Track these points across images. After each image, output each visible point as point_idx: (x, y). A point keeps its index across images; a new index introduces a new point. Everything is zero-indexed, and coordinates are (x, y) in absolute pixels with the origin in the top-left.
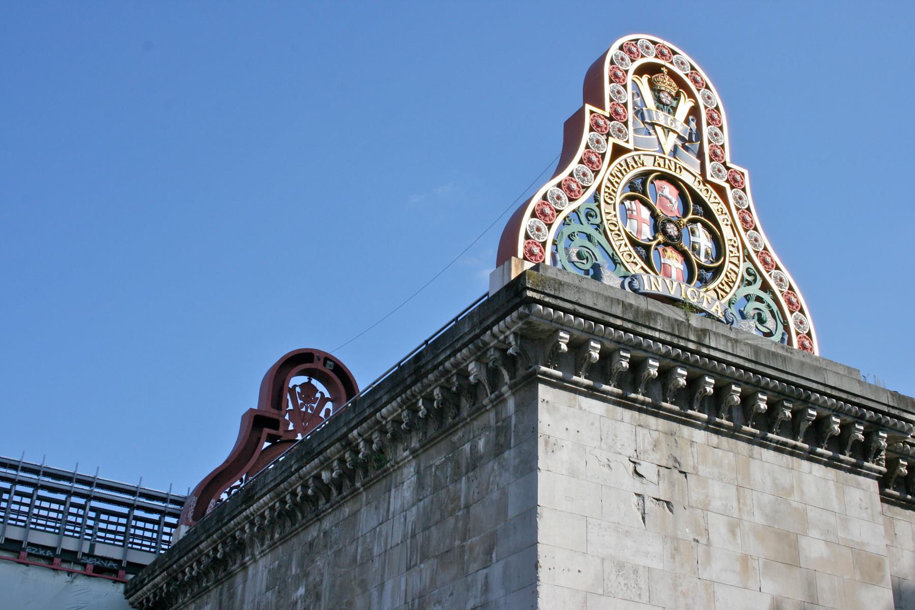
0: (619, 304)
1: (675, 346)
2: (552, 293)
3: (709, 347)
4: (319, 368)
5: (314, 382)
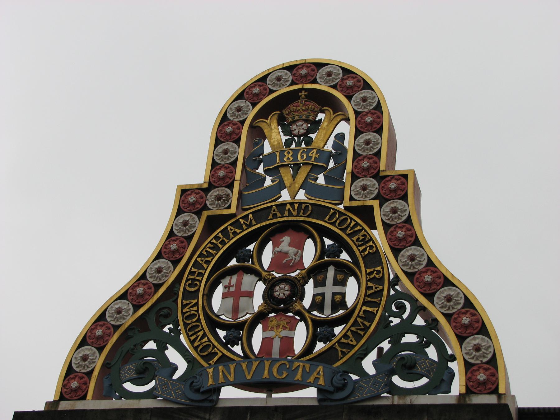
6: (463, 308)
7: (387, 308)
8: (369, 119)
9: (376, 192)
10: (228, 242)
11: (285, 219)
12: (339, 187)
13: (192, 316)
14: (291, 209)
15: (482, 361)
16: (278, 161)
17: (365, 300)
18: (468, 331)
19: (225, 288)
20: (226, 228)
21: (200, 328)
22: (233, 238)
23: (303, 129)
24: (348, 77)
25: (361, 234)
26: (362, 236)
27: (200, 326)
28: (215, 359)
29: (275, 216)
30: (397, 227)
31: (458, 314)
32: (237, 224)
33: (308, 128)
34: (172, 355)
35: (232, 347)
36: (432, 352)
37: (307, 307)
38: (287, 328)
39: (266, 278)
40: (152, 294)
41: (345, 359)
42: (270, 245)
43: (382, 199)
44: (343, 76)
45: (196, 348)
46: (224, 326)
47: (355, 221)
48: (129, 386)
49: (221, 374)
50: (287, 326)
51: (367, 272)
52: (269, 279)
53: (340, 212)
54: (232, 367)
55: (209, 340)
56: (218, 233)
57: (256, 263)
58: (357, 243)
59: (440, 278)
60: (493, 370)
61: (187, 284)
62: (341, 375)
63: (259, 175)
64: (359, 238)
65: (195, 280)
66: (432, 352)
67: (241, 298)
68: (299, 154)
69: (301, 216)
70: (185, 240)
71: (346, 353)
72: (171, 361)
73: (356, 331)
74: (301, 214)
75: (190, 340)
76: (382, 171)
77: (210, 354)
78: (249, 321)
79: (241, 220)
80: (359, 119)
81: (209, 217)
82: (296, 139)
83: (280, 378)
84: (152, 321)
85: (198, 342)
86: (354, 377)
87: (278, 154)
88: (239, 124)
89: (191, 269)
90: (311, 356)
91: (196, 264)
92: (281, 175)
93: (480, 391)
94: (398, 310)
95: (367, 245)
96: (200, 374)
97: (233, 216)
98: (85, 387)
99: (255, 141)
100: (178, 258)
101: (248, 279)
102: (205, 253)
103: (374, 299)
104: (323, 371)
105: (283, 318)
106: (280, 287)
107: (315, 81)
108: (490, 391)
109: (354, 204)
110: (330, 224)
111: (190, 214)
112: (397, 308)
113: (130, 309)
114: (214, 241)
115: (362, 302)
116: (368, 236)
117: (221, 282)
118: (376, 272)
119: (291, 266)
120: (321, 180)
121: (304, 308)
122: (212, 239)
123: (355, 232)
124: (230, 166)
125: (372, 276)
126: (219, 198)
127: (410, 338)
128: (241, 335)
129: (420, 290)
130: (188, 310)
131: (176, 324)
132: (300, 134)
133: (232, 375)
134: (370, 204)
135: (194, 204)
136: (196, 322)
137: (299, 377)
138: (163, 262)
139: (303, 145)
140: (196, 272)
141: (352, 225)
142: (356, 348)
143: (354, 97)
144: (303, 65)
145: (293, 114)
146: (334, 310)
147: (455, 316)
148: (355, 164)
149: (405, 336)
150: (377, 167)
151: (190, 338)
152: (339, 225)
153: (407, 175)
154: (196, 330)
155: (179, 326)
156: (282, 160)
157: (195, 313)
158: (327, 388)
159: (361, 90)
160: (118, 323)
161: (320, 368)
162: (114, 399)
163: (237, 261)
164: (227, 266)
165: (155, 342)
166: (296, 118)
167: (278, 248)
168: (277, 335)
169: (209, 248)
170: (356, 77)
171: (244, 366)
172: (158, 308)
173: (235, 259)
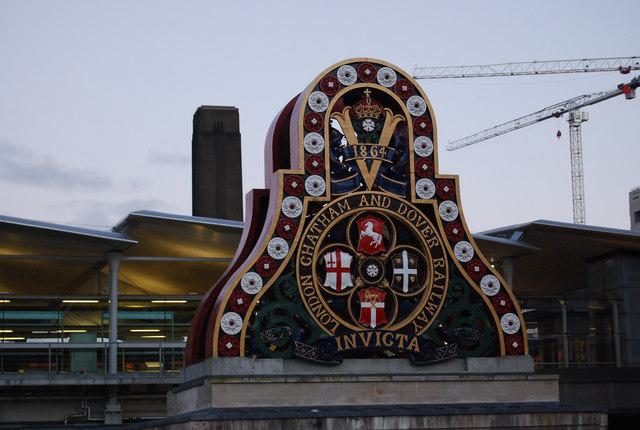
13: (310, 291)
54: (354, 336)
67: (343, 274)
81: (311, 204)
84: (277, 291)
91: (307, 241)
109: (418, 201)
156: (359, 154)
171: (362, 335)
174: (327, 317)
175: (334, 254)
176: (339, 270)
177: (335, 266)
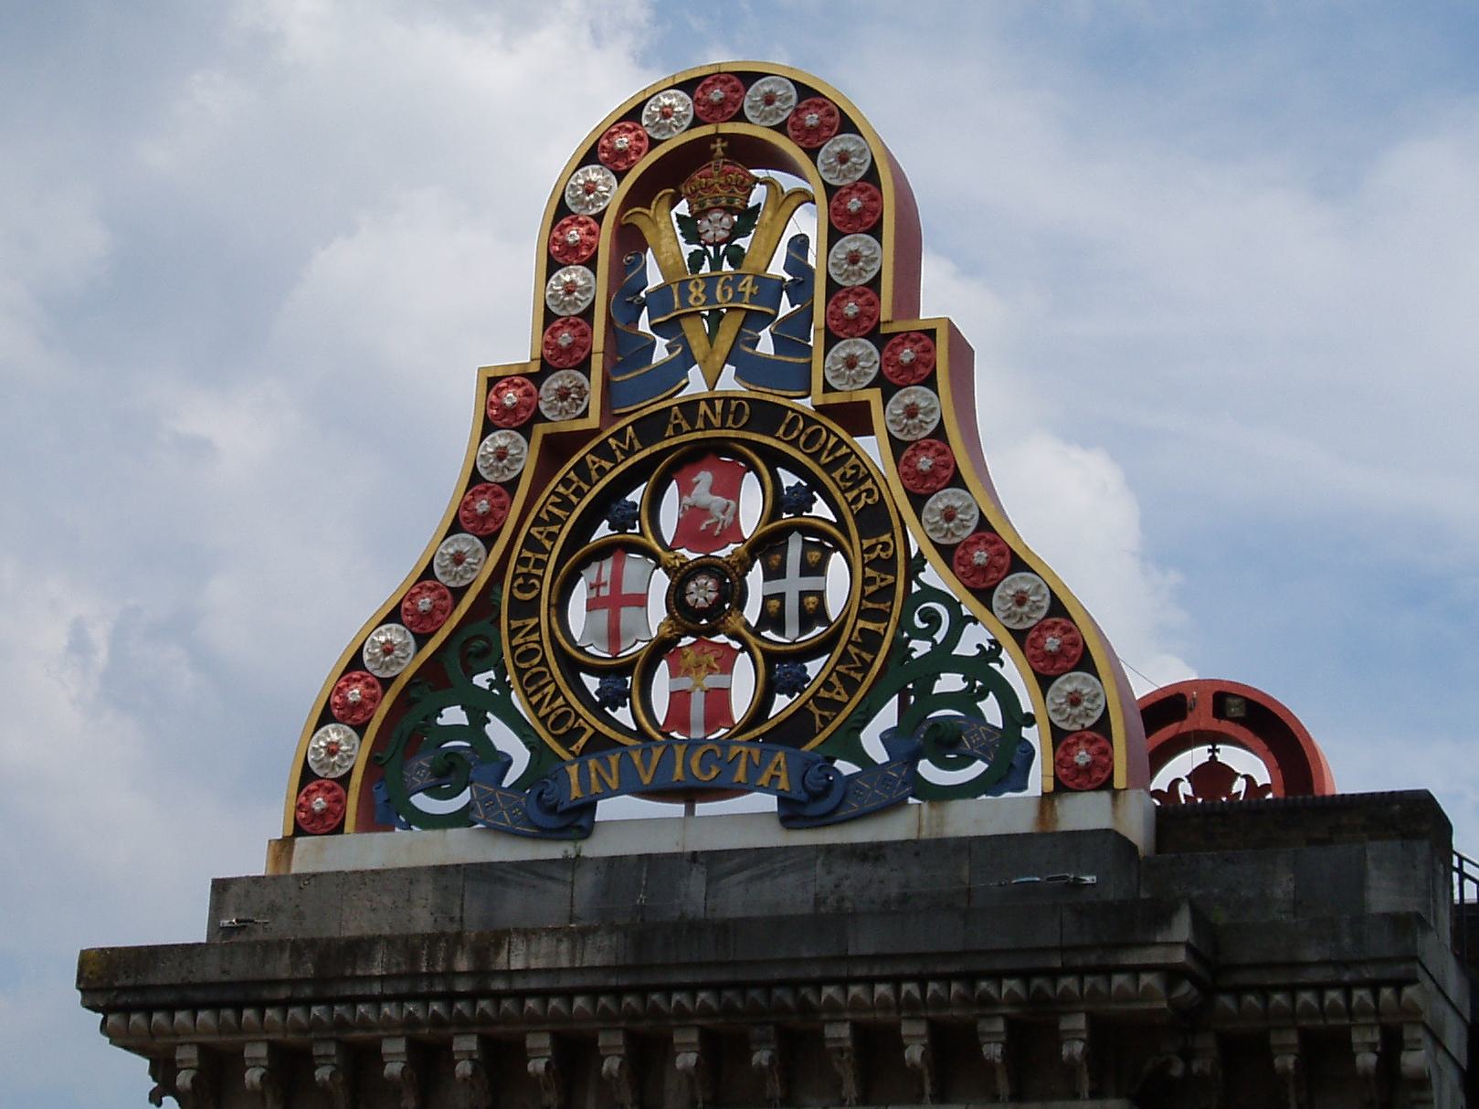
0: (282, 950)
1: (425, 999)
2: (130, 982)
3: (509, 974)
4: (1202, 725)
5: (1231, 756)
6: (1047, 617)
7: (904, 623)
8: (854, 204)
9: (874, 372)
10: (589, 491)
11: (699, 435)
12: (802, 360)
14: (709, 412)
15: (1083, 726)
16: (676, 306)
17: (862, 608)
18: (1058, 666)
19: (592, 588)
20: (583, 458)
21: (548, 678)
22: (598, 481)
23: (723, 229)
24: (809, 104)
25: (848, 464)
26: (852, 468)
27: (548, 674)
28: (582, 741)
29: (678, 430)
30: (917, 447)
31: (1039, 630)
32: (603, 451)
33: (734, 225)
34: (500, 734)
35: (614, 710)
36: (991, 709)
37: (753, 624)
38: (716, 669)
39: (669, 566)
40: (449, 611)
41: (827, 732)
42: (673, 488)
43: (886, 385)
44: (799, 101)
45: (543, 720)
46: (592, 671)
47: (836, 435)
48: (422, 801)
49: (593, 775)
50: (715, 665)
51: (865, 547)
52: (675, 566)
53: (806, 417)
55: (568, 704)
56: (568, 473)
57: (650, 535)
58: (841, 484)
59: (1003, 555)
60: (1104, 744)
61: (515, 585)
62: (820, 768)
63: (643, 336)
64: (845, 473)
65: (527, 576)
66: (991, 709)
67: (624, 611)
68: (719, 287)
69: (730, 428)
70: (503, 491)
71: (830, 719)
72: (499, 748)
73: (846, 672)
74: (730, 423)
75: (530, 703)
76: (884, 323)
77: (571, 730)
78: (641, 659)
79: (611, 440)
80: (834, 203)
81: (546, 437)
82: (711, 249)
83: (706, 779)
84: (453, 664)
85: (547, 707)
86: (846, 767)
87: (675, 288)
88: (594, 225)
89: (520, 553)
90: (765, 728)
91: (531, 543)
92: (684, 336)
93: (1078, 785)
94: (926, 625)
95: (862, 488)
96: (554, 776)
97: (593, 433)
98: (339, 808)
99: (629, 258)
100: (494, 530)
101: (634, 565)
102: (546, 517)
103: (880, 603)
104: (786, 762)
105: (707, 649)
106: (697, 584)
107: (740, 117)
108: (1100, 783)
109: (833, 399)
110: (788, 442)
111: (508, 431)
112: (923, 620)
113: (408, 644)
114: (561, 489)
115: (856, 612)
116: (863, 469)
117: (581, 575)
118: (880, 546)
119: (717, 536)
120: (766, 345)
121: (747, 624)
122: (556, 487)
123: (836, 459)
124: (579, 320)
125: (873, 556)
126: (563, 394)
127: (950, 682)
128: (629, 687)
129: (965, 581)
130: (522, 641)
131: (502, 672)
132: (717, 240)
133: (615, 777)
134: (864, 399)
135: (514, 410)
136: (538, 665)
137: (740, 775)
138: (464, 539)
139: (726, 267)
140: (530, 558)
141: (830, 445)
142: (848, 709)
143: (821, 152)
144: (715, 76)
145: (700, 196)
146: (805, 626)
147: (1032, 635)
148: (831, 307)
149: (940, 678)
150: (874, 314)
151: (531, 699)
152: (805, 443)
153: (934, 330)
154: (541, 683)
155: (507, 674)
156: (684, 303)
157: (536, 646)
158: (794, 795)
159: (835, 135)
160: (388, 675)
161: (780, 756)
162: (397, 830)
163: (611, 528)
164: (593, 539)
165: (463, 709)
166: (709, 204)
167: (690, 496)
168: (699, 685)
169: (552, 504)
170: (825, 104)
171: (636, 757)
172: (465, 638)
173: (606, 523)
174: (567, 714)
175: (608, 566)
176: (614, 601)
177: (605, 592)
